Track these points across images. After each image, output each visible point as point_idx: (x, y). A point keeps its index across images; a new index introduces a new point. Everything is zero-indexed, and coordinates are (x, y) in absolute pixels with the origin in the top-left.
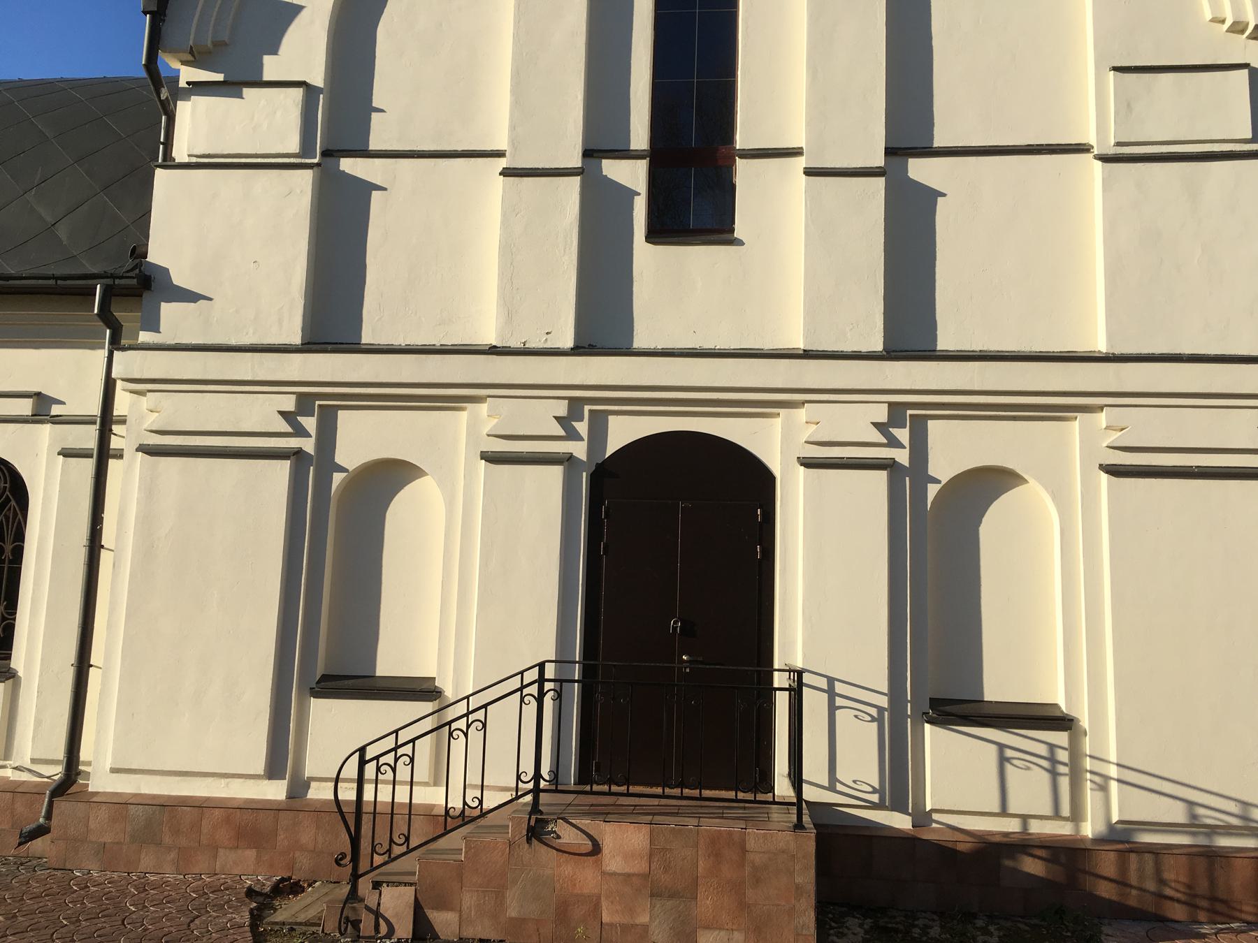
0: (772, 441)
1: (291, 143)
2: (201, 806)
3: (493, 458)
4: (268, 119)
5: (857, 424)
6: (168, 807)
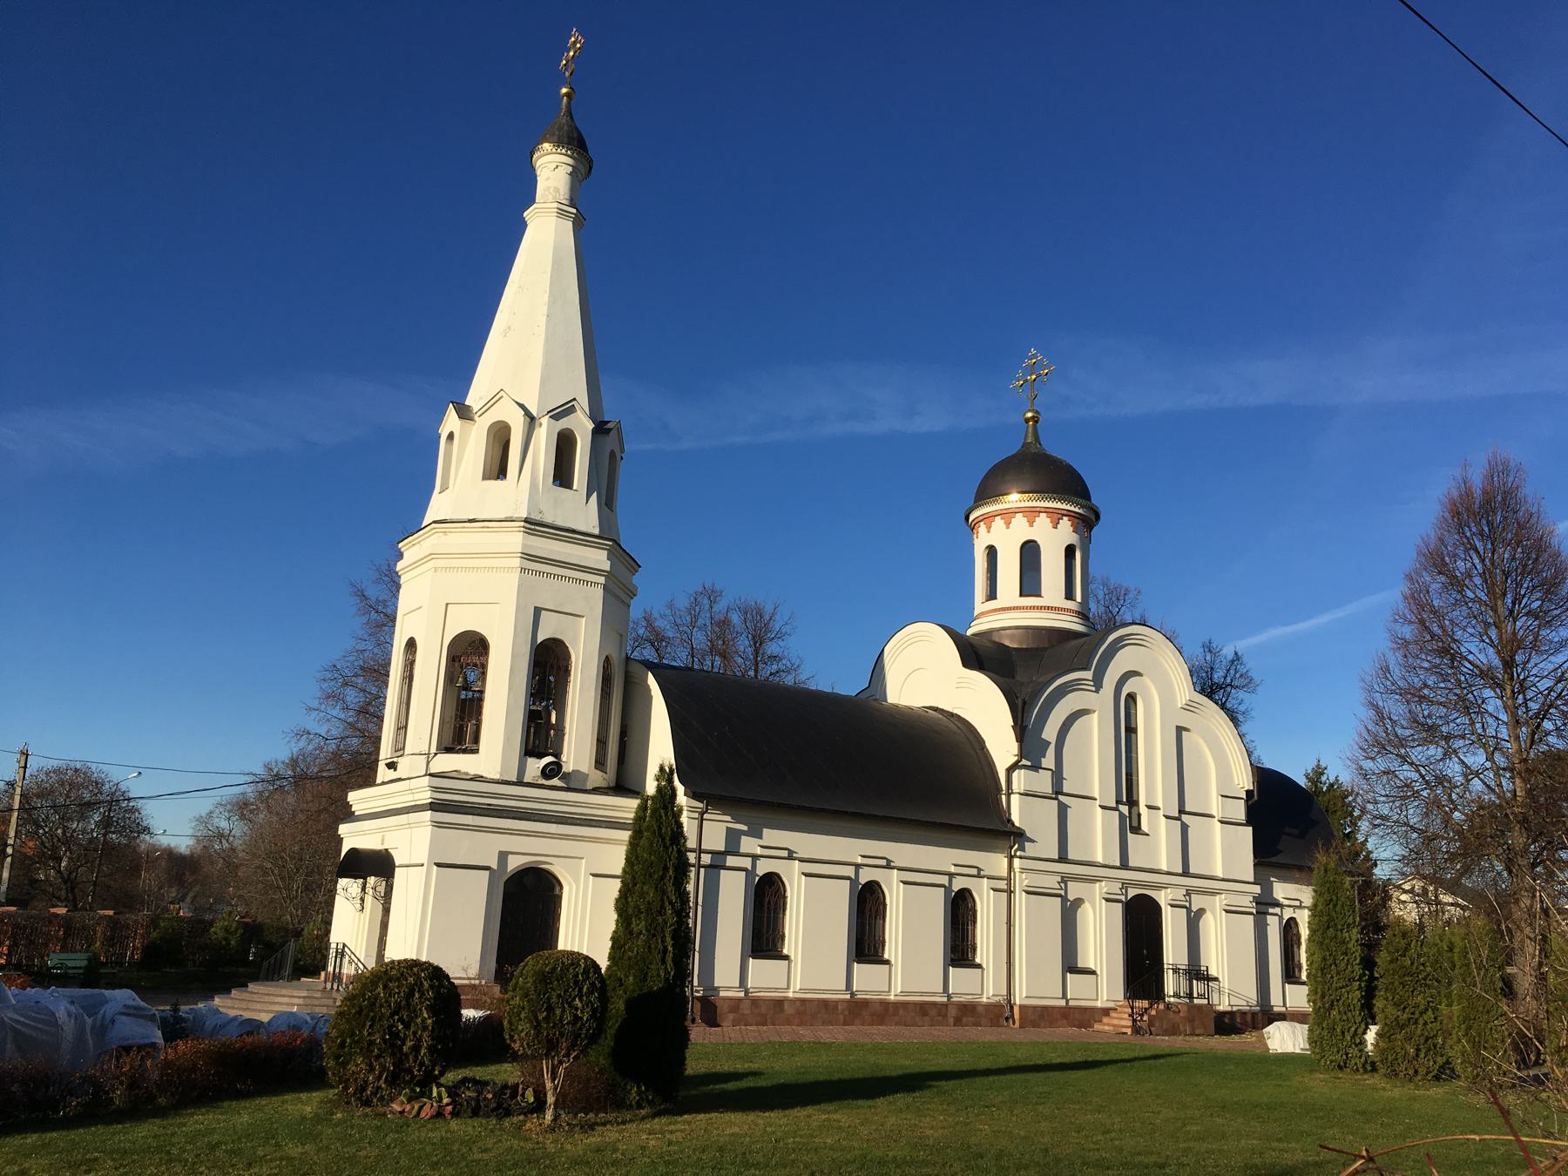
0: (1162, 898)
1: (1049, 790)
2: (1053, 1008)
3: (1107, 900)
4: (1043, 781)
5: (1179, 894)
6: (1045, 1008)
